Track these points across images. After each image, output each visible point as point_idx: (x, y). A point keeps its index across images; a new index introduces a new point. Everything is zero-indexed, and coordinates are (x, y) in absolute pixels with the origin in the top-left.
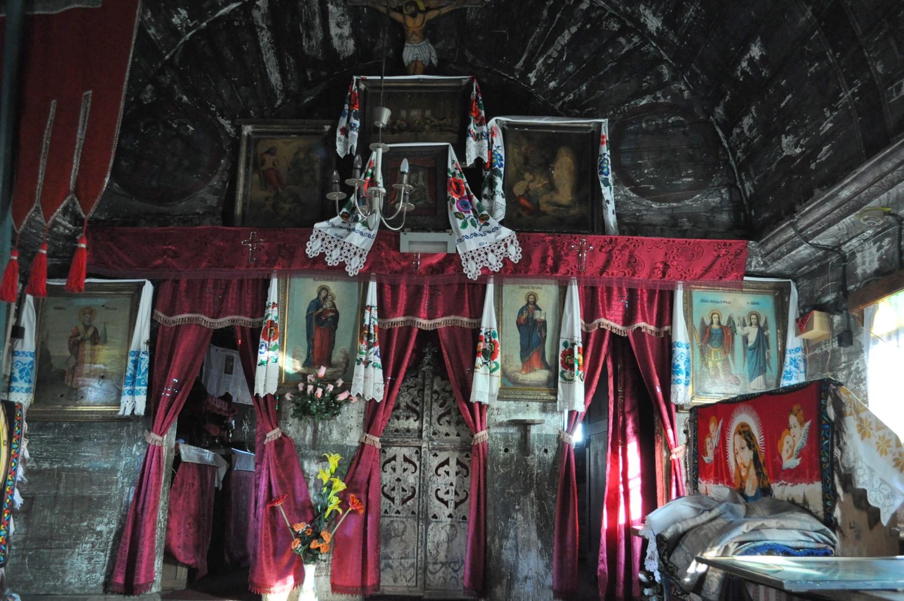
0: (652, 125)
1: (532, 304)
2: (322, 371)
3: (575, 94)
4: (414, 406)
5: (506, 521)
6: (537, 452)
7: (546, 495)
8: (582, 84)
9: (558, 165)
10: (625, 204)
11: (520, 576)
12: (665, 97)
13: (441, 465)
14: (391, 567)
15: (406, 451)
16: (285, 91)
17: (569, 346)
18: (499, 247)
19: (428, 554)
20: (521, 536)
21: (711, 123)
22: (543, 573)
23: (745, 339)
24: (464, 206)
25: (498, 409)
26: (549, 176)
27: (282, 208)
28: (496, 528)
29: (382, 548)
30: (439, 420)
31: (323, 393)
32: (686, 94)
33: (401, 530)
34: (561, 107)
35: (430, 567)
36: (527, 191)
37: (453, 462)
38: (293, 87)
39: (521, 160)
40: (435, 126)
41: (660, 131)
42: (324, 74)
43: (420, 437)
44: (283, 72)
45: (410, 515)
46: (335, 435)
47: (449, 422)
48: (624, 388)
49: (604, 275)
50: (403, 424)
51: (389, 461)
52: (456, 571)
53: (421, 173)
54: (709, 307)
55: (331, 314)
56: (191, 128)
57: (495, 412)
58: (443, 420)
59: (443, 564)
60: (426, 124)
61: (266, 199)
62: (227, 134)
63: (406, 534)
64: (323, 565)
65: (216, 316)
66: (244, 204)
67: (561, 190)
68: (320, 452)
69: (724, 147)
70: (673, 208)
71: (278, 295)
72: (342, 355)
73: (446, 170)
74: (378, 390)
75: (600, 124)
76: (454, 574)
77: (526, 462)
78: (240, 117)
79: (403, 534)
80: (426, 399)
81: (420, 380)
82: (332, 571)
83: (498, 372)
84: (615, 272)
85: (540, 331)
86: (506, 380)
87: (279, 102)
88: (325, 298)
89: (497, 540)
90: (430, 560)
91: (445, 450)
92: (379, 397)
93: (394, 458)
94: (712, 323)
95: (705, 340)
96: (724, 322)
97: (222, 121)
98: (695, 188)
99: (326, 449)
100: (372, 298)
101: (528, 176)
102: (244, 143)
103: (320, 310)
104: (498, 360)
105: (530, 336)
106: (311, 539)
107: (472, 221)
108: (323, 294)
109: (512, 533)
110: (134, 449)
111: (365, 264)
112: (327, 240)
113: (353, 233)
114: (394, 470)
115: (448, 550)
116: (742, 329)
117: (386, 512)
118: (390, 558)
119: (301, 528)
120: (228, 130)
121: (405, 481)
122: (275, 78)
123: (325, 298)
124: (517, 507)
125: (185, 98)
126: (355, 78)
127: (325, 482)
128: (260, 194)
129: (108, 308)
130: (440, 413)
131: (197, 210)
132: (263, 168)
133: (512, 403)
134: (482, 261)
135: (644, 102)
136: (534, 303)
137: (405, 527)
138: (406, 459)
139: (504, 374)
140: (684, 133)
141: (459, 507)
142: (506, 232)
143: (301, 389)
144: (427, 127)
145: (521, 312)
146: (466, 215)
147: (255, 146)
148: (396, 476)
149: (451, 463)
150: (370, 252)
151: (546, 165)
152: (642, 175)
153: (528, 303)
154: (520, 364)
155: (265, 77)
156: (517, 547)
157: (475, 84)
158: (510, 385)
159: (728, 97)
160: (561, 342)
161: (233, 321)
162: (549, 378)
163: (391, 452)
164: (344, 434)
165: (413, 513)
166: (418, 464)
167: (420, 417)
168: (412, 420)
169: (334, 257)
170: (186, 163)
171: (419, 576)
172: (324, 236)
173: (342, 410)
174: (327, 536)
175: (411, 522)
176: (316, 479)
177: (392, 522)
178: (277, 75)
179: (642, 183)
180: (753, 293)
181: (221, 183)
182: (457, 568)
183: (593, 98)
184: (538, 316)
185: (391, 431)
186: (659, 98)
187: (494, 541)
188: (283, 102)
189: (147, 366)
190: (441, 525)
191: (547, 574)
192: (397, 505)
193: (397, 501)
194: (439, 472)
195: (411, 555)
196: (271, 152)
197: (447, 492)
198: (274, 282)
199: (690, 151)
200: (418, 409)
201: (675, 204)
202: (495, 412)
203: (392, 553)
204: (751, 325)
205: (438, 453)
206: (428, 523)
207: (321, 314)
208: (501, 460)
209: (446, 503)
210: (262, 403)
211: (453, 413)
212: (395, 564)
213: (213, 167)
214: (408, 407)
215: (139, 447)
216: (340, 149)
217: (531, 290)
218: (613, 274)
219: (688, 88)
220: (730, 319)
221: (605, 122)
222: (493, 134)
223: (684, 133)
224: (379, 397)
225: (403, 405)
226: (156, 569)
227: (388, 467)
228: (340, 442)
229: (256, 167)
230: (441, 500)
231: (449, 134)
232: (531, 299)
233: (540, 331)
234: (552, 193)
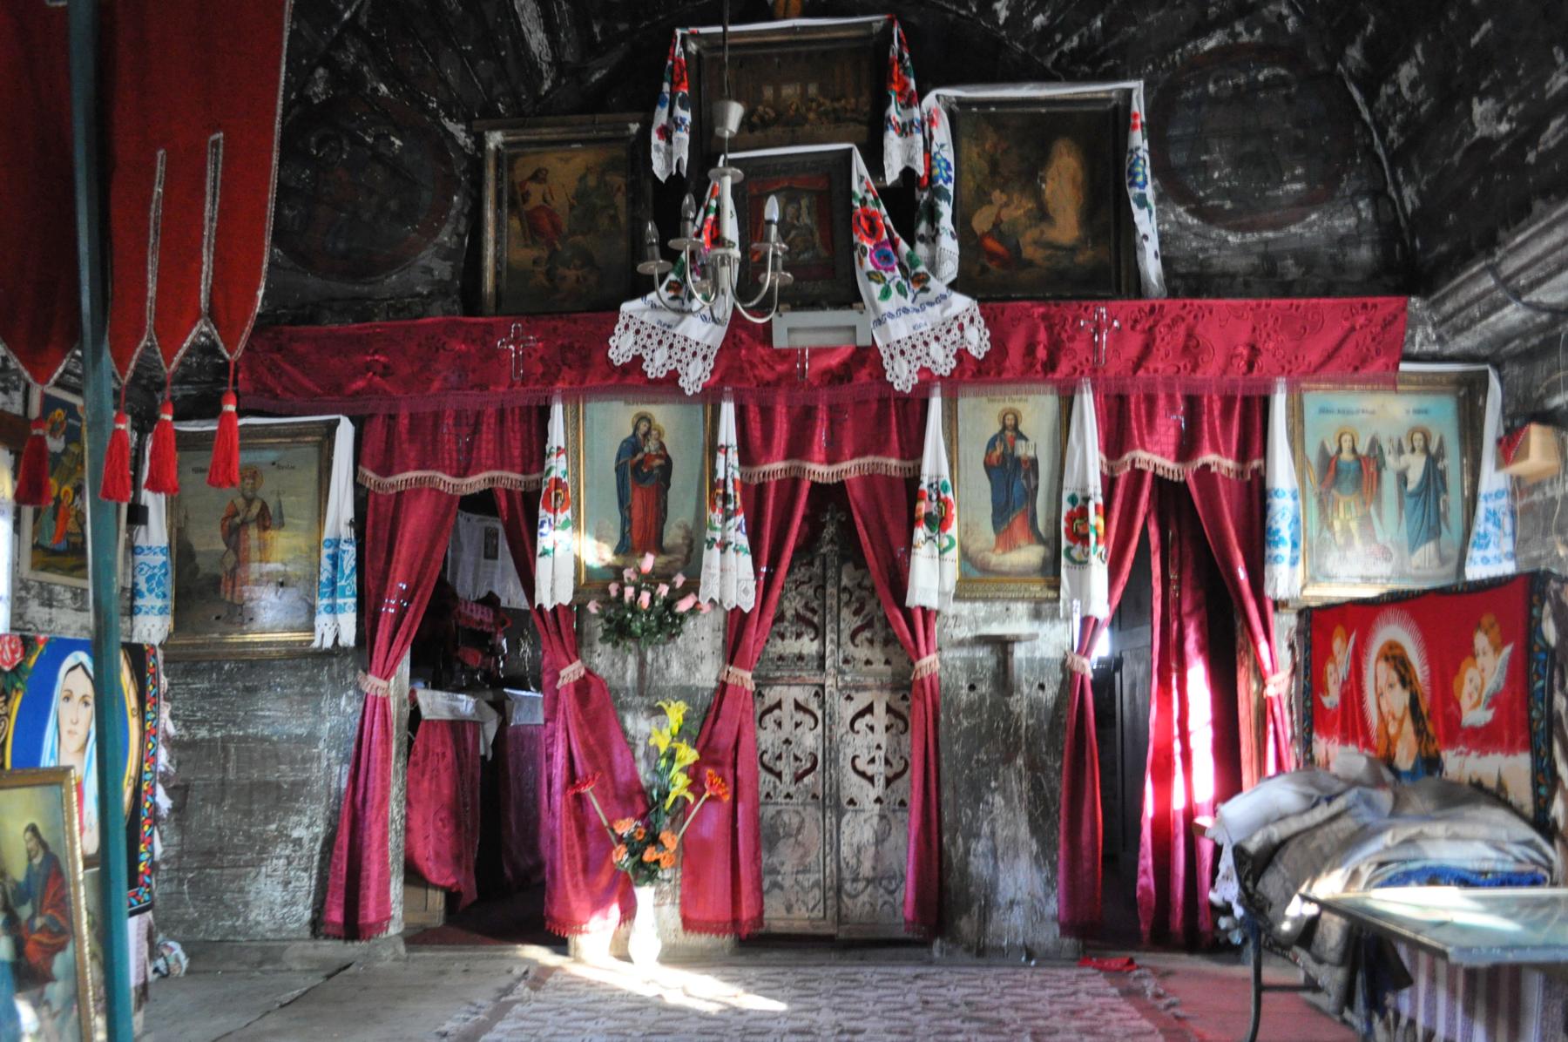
0: (1226, 87)
1: (1011, 430)
2: (648, 562)
3: (1081, 37)
4: (809, 615)
5: (975, 809)
6: (1025, 689)
7: (1044, 763)
8: (1095, 16)
9: (1051, 172)
10: (1177, 237)
11: (1003, 897)
12: (1250, 31)
13: (861, 714)
14: (781, 888)
15: (798, 693)
16: (557, 63)
17: (1080, 502)
18: (949, 331)
19: (843, 864)
20: (1002, 833)
21: (1340, 77)
22: (1041, 894)
23: (1402, 478)
24: (884, 259)
25: (956, 617)
26: (1038, 195)
27: (564, 278)
28: (958, 821)
29: (764, 856)
30: (853, 636)
31: (652, 599)
32: (1291, 23)
33: (795, 826)
34: (1056, 63)
35: (848, 886)
36: (997, 225)
37: (880, 709)
38: (569, 55)
39: (984, 166)
40: (826, 113)
41: (1244, 97)
42: (623, 27)
43: (822, 667)
44: (550, 29)
45: (809, 800)
46: (676, 670)
47: (871, 642)
48: (1180, 572)
49: (1141, 373)
50: (791, 646)
51: (770, 710)
52: (892, 893)
53: (804, 202)
54: (1335, 421)
55: (658, 462)
56: (398, 142)
57: (951, 622)
58: (858, 641)
59: (869, 881)
60: (809, 109)
61: (535, 262)
62: (461, 148)
63: (805, 832)
64: (666, 887)
65: (463, 472)
66: (497, 274)
67: (1060, 220)
68: (650, 696)
69: (1363, 122)
70: (1267, 242)
71: (566, 432)
72: (681, 533)
73: (850, 194)
74: (746, 591)
75: (1129, 92)
76: (887, 897)
77: (1007, 706)
78: (481, 116)
79: (799, 830)
80: (828, 603)
81: (817, 569)
82: (682, 897)
83: (954, 553)
84: (1160, 366)
85: (1027, 477)
86: (968, 566)
87: (547, 85)
88: (647, 435)
89: (960, 841)
90: (847, 874)
91: (865, 688)
92: (748, 603)
93: (778, 705)
94: (1340, 450)
96: (1363, 448)
97: (451, 126)
99: (661, 693)
100: (728, 432)
101: (997, 195)
102: (491, 163)
103: (639, 456)
104: (953, 530)
105: (1009, 486)
106: (643, 846)
107: (899, 285)
108: (643, 427)
109: (986, 829)
110: (343, 702)
111: (712, 372)
112: (644, 333)
113: (689, 318)
114: (779, 725)
115: (877, 857)
116: (1397, 459)
117: (768, 795)
118: (778, 873)
119: (626, 827)
120: (461, 142)
121: (799, 745)
122: (537, 40)
123: (647, 435)
124: (993, 784)
125: (383, 88)
126: (679, 32)
127: (663, 750)
128: (523, 255)
129: (279, 467)
130: (854, 626)
131: (418, 289)
132: (527, 208)
133: (979, 605)
134: (919, 358)
135: (1210, 44)
136: (1015, 428)
137: (803, 821)
138: (798, 706)
139: (965, 555)
141: (893, 786)
142: (961, 303)
143: (614, 593)
144: (812, 116)
145: (992, 444)
146: (888, 276)
147: (511, 169)
148: (783, 734)
149: (876, 710)
150: (720, 350)
151: (1030, 176)
152: (1208, 181)
153: (1005, 428)
154: (992, 536)
155: (520, 41)
156: (994, 851)
157: (896, 30)
158: (975, 574)
159: (1370, 28)
160: (1065, 495)
161: (492, 480)
162: (1044, 560)
163: (772, 695)
164: (690, 667)
165: (814, 796)
166: (819, 714)
167: (819, 633)
168: (806, 639)
169: (658, 363)
170: (393, 205)
171: (829, 902)
172: (638, 325)
173: (685, 627)
174: (670, 840)
175: (811, 813)
176: (647, 744)
177: (779, 812)
178: (541, 35)
179: (1208, 197)
180: (1417, 392)
181: (455, 239)
182: (893, 886)
183: (1115, 41)
184: (1022, 450)
185: (772, 660)
186: (1240, 34)
187: (954, 842)
188: (555, 83)
189: (353, 563)
190: (862, 817)
191: (1047, 896)
192: (787, 784)
193: (787, 778)
194: (857, 726)
195: (814, 867)
196: (538, 176)
197: (872, 761)
198: (557, 411)
199: (1300, 133)
200: (816, 619)
201: (1270, 235)
202: (951, 622)
203: (782, 864)
204: (1413, 450)
205: (853, 694)
206: (840, 814)
207: (641, 462)
208: (963, 705)
209: (871, 779)
210: (549, 618)
211: (878, 626)
212: (788, 882)
213: (440, 211)
214: (799, 617)
215: (350, 699)
216: (659, 168)
217: (1008, 405)
218: (1156, 371)
220: (1374, 443)
221: (1137, 86)
222: (932, 121)
223: (1288, 99)
224: (748, 603)
225: (789, 613)
226: (392, 897)
227: (769, 720)
228: (684, 682)
229: (513, 204)
230: (863, 774)
231: (852, 127)
232: (1010, 420)
233: (1027, 477)
234: (1044, 226)
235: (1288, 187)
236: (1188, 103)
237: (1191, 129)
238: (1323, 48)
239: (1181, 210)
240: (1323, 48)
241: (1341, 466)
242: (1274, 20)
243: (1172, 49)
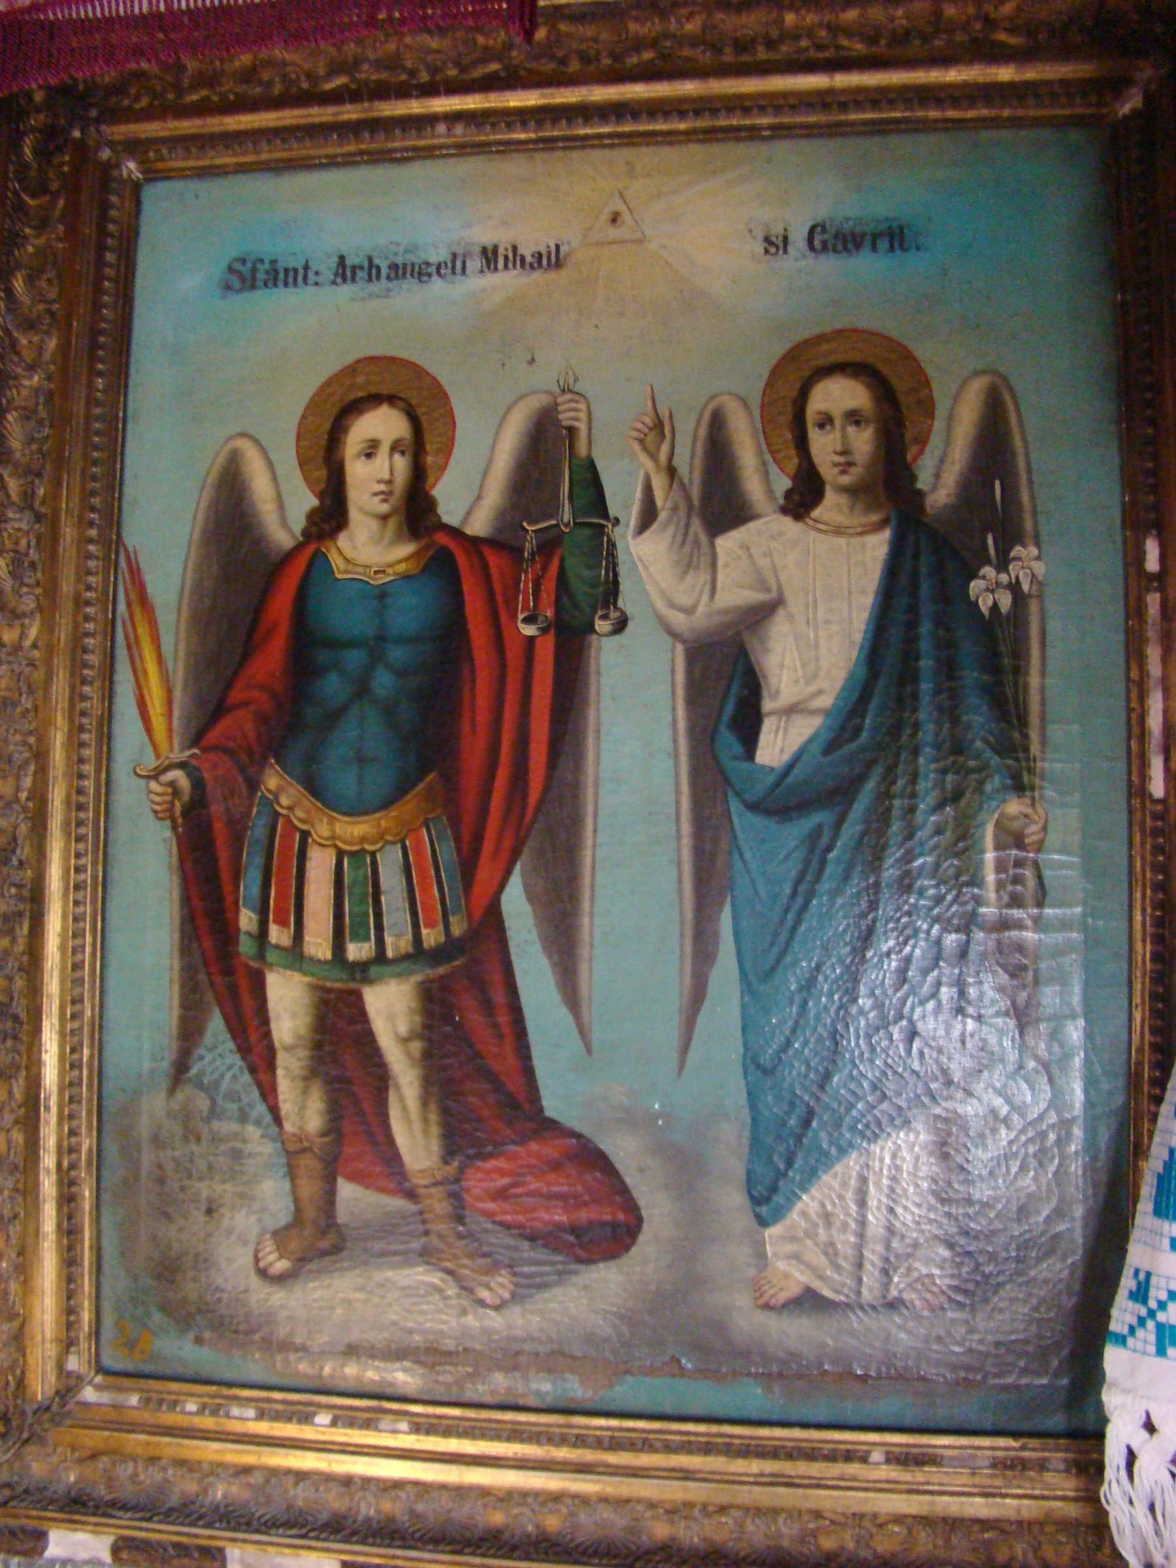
23: (725, 681)
54: (320, 331)
94: (331, 515)
95: (240, 725)
96: (470, 495)
116: (696, 558)
204: (803, 497)
220: (551, 457)
241: (344, 618)
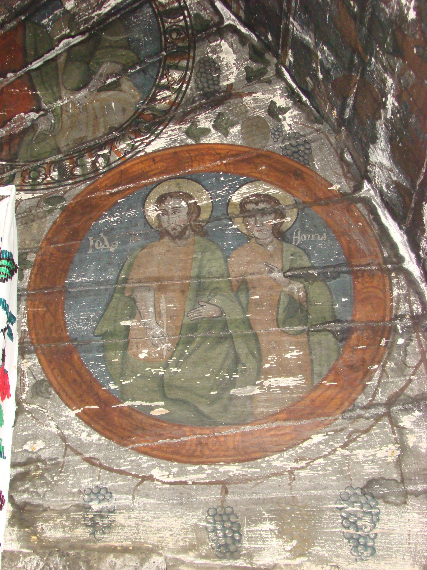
0: (175, 210)
10: (56, 466)
12: (222, 126)
21: (367, 202)
69: (408, 274)
70: (225, 485)
98: (305, 411)
135: (158, 144)
140: (279, 234)
159: (391, 101)
186: (206, 132)
199: (296, 288)
201: (234, 469)
219: (298, 103)
223: (279, 234)
235: (273, 381)
236: (110, 231)
237: (111, 274)
238: (342, 159)
239: (70, 413)
240: (342, 159)
242: (262, 113)
243: (93, 149)
